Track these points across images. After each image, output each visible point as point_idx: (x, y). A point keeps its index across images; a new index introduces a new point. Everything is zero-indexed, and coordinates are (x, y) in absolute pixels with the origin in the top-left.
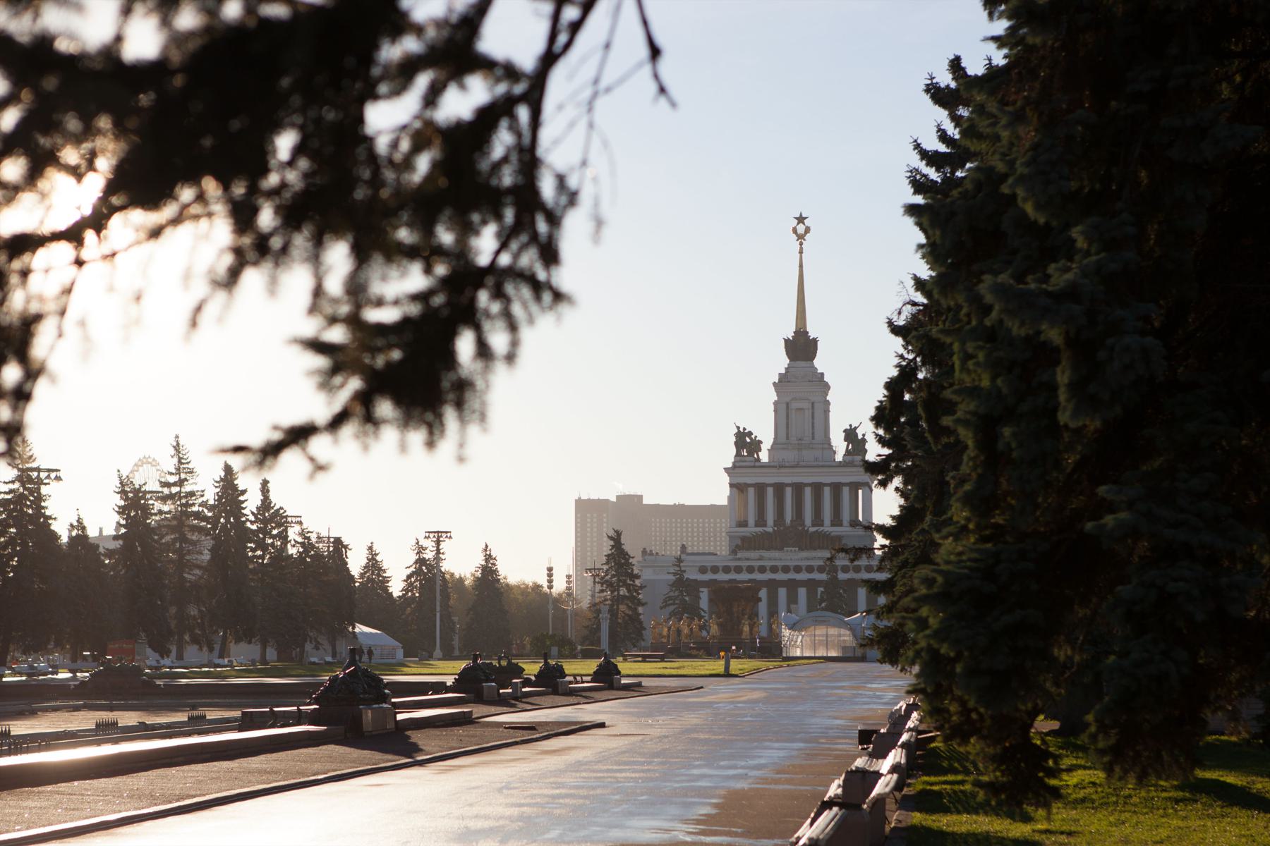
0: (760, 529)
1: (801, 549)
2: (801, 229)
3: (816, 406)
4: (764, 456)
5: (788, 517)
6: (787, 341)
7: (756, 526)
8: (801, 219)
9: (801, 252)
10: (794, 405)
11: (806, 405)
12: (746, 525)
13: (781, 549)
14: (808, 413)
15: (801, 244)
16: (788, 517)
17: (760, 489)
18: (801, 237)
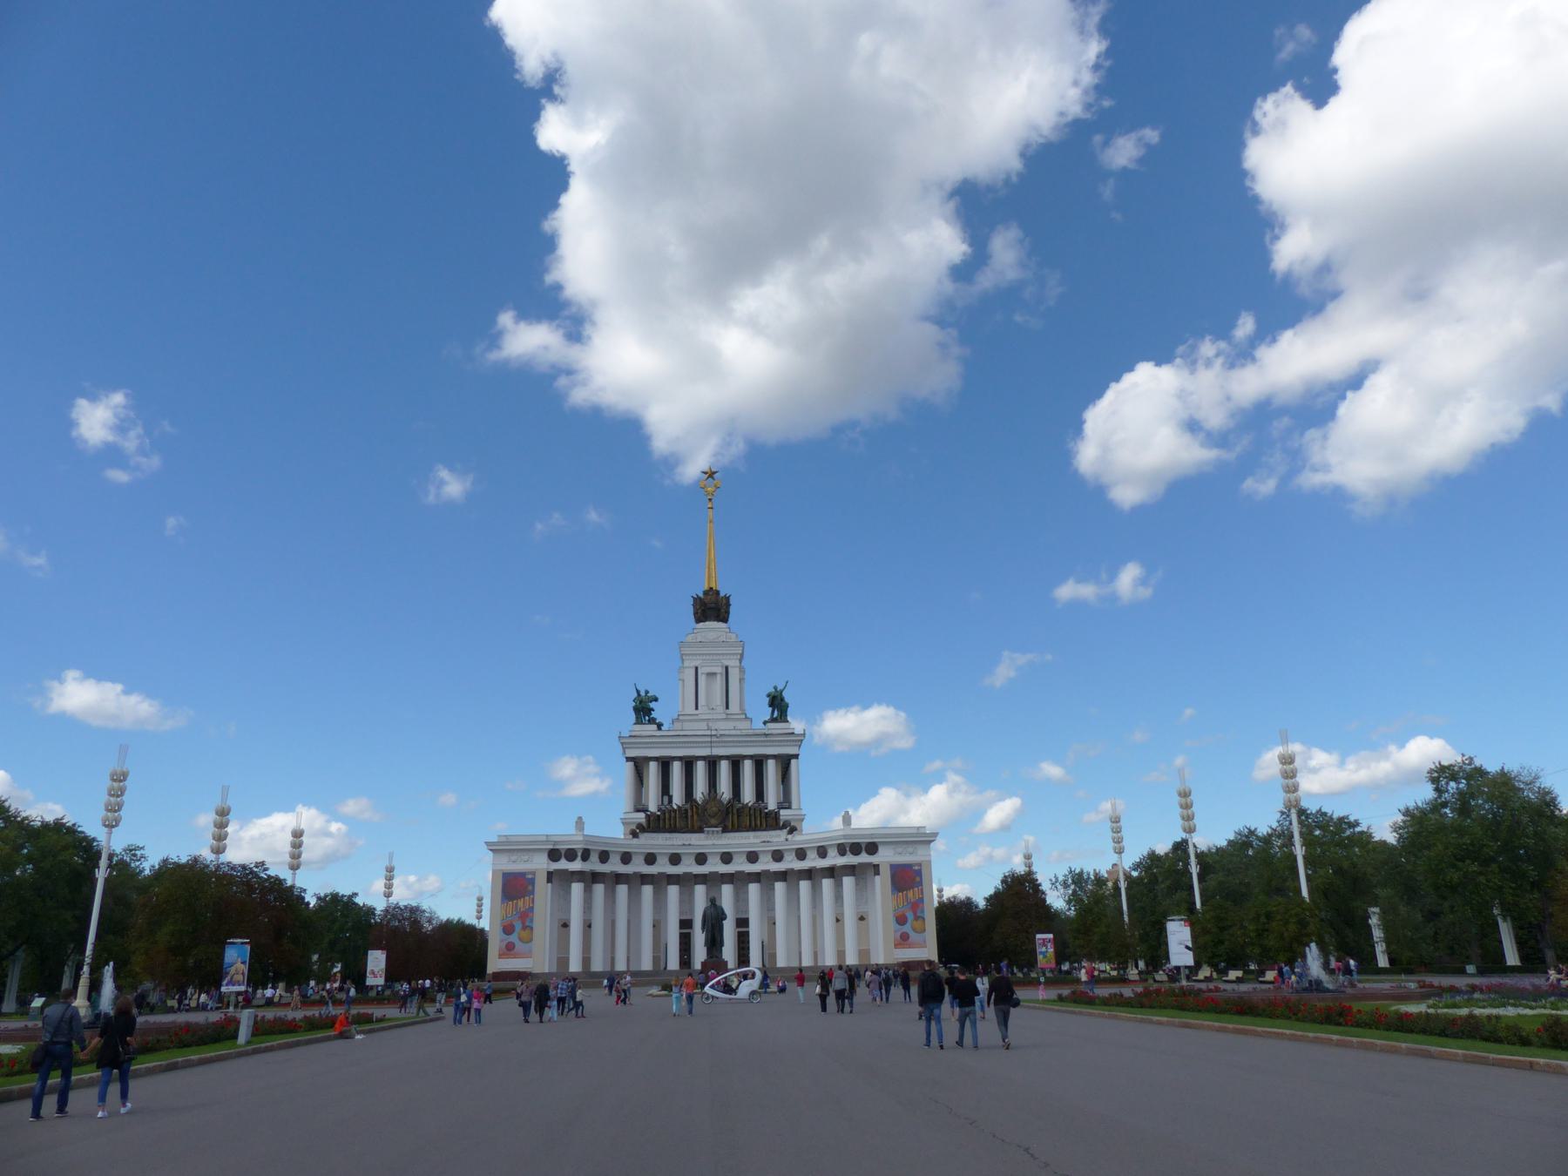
1: (725, 830)
13: (700, 830)
14: (720, 681)
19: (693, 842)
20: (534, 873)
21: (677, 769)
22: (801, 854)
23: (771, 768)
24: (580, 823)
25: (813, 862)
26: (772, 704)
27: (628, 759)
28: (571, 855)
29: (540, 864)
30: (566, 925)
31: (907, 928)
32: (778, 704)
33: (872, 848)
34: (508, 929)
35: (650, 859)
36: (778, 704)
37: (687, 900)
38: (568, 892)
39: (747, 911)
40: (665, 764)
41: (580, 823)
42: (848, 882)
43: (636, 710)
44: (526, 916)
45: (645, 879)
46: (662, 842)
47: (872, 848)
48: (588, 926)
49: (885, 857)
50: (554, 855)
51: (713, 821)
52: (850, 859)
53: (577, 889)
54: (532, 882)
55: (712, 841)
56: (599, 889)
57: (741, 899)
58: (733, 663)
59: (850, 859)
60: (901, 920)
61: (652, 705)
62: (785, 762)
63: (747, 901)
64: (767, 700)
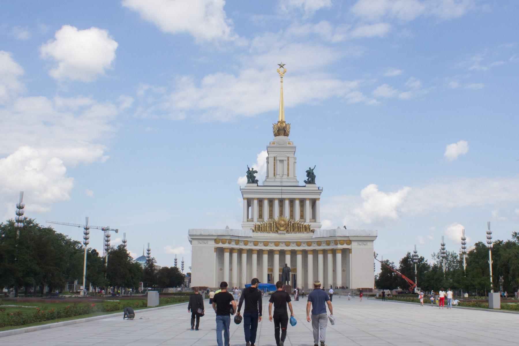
3: (290, 159)
10: (278, 158)
14: (286, 163)
17: (261, 201)
22: (319, 243)
23: (308, 204)
26: (308, 176)
27: (244, 199)
32: (311, 177)
36: (311, 177)
39: (296, 266)
40: (261, 201)
42: (339, 256)
43: (248, 176)
47: (349, 242)
51: (282, 228)
52: (340, 247)
53: (227, 255)
57: (294, 261)
58: (291, 155)
59: (340, 247)
61: (255, 175)
62: (314, 202)
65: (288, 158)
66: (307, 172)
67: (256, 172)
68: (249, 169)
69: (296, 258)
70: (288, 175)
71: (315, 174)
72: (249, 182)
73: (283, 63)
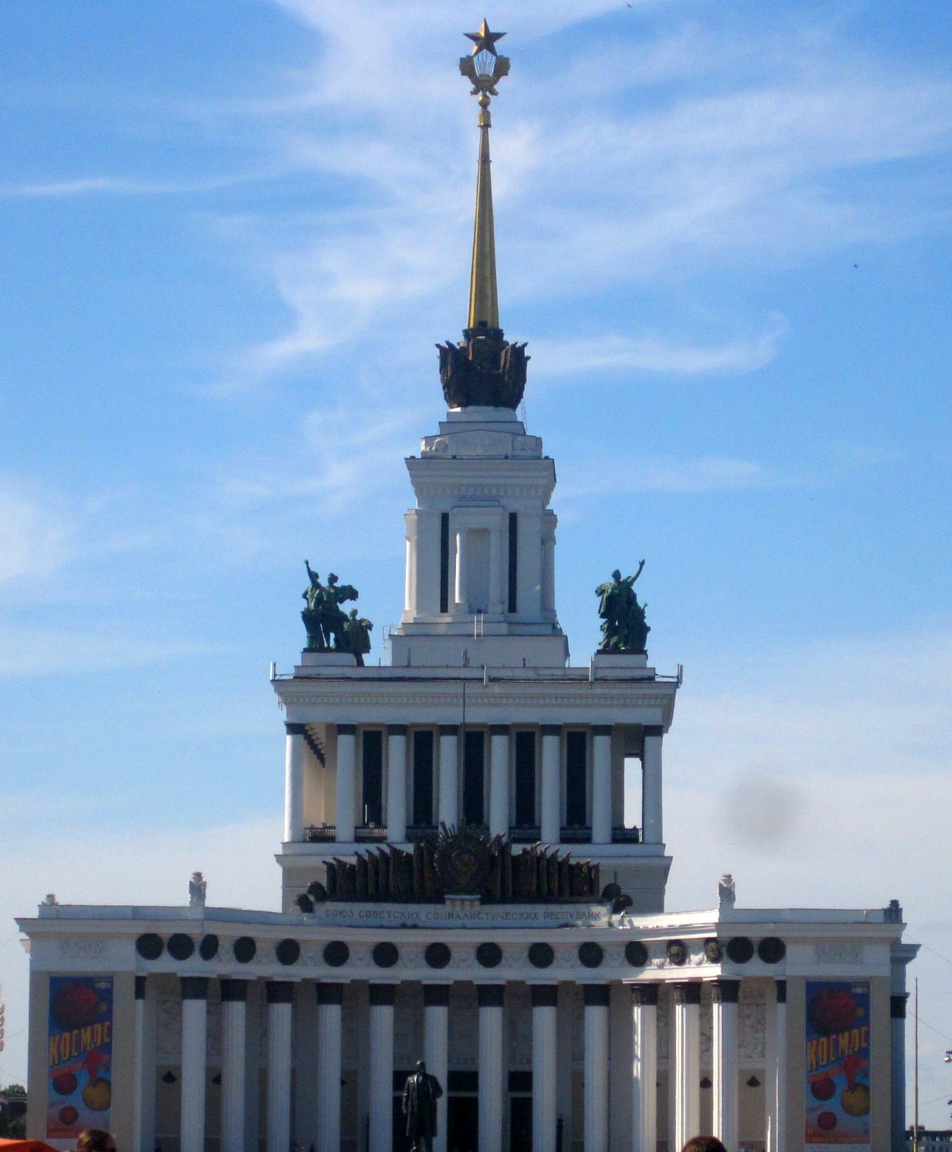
0: (373, 848)
1: (488, 899)
2: (485, 64)
4: (379, 655)
5: (447, 811)
6: (449, 355)
7: (358, 839)
8: (487, 41)
9: (486, 126)
11: (495, 521)
12: (332, 839)
13: (438, 899)
14: (497, 546)
15: (484, 104)
16: (447, 811)
18: (484, 86)
19: (423, 920)
20: (110, 979)
21: (397, 753)
22: (637, 953)
24: (198, 888)
25: (658, 971)
27: (294, 728)
28: (181, 946)
29: (122, 960)
30: (170, 1078)
31: (833, 1105)
33: (773, 949)
34: (63, 1084)
35: (336, 953)
36: (623, 617)
37: (410, 1037)
38: (178, 1015)
39: (529, 1061)
40: (372, 744)
41: (198, 888)
43: (308, 617)
44: (98, 1061)
45: (327, 993)
46: (362, 927)
48: (215, 1079)
49: (799, 964)
50: (149, 946)
54: (107, 996)
55: (463, 925)
56: (237, 1010)
60: (822, 1089)
61: (346, 607)
63: (529, 1037)
64: (596, 602)
65: (513, 518)
66: (600, 592)
67: (351, 594)
68: (313, 576)
69: (529, 1022)
70: (512, 608)
71: (640, 602)
72: (316, 645)
73: (493, 29)
